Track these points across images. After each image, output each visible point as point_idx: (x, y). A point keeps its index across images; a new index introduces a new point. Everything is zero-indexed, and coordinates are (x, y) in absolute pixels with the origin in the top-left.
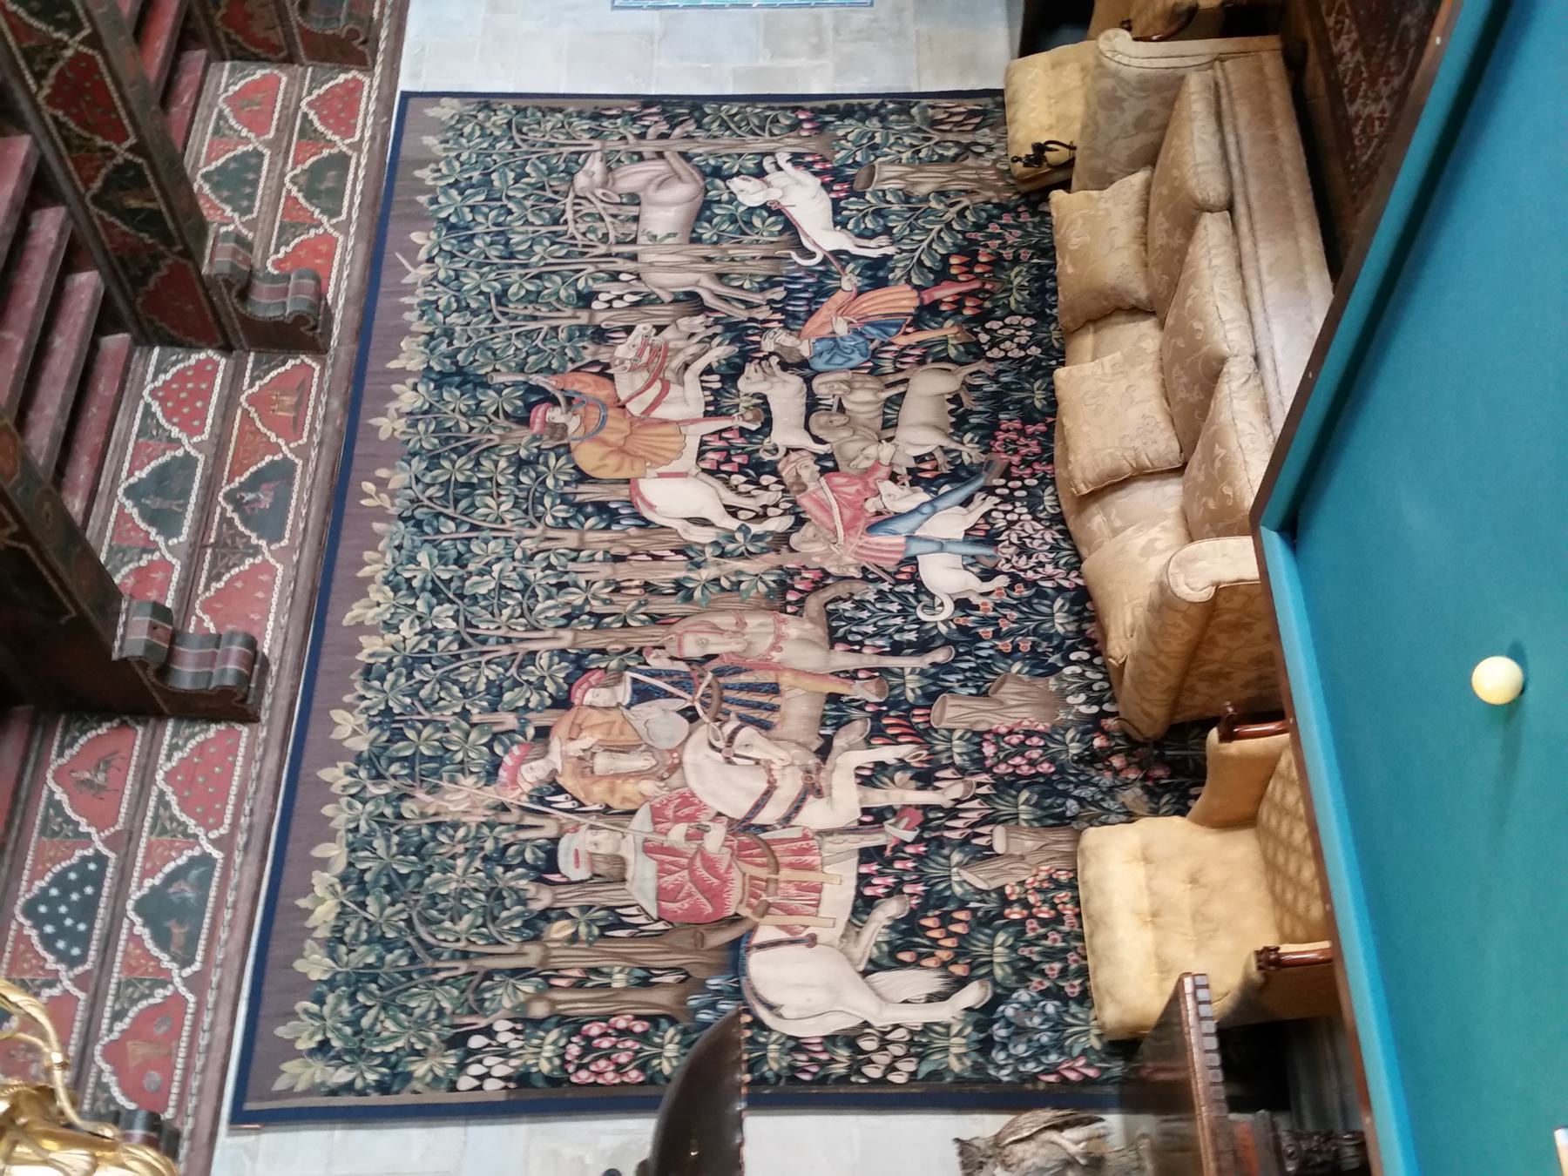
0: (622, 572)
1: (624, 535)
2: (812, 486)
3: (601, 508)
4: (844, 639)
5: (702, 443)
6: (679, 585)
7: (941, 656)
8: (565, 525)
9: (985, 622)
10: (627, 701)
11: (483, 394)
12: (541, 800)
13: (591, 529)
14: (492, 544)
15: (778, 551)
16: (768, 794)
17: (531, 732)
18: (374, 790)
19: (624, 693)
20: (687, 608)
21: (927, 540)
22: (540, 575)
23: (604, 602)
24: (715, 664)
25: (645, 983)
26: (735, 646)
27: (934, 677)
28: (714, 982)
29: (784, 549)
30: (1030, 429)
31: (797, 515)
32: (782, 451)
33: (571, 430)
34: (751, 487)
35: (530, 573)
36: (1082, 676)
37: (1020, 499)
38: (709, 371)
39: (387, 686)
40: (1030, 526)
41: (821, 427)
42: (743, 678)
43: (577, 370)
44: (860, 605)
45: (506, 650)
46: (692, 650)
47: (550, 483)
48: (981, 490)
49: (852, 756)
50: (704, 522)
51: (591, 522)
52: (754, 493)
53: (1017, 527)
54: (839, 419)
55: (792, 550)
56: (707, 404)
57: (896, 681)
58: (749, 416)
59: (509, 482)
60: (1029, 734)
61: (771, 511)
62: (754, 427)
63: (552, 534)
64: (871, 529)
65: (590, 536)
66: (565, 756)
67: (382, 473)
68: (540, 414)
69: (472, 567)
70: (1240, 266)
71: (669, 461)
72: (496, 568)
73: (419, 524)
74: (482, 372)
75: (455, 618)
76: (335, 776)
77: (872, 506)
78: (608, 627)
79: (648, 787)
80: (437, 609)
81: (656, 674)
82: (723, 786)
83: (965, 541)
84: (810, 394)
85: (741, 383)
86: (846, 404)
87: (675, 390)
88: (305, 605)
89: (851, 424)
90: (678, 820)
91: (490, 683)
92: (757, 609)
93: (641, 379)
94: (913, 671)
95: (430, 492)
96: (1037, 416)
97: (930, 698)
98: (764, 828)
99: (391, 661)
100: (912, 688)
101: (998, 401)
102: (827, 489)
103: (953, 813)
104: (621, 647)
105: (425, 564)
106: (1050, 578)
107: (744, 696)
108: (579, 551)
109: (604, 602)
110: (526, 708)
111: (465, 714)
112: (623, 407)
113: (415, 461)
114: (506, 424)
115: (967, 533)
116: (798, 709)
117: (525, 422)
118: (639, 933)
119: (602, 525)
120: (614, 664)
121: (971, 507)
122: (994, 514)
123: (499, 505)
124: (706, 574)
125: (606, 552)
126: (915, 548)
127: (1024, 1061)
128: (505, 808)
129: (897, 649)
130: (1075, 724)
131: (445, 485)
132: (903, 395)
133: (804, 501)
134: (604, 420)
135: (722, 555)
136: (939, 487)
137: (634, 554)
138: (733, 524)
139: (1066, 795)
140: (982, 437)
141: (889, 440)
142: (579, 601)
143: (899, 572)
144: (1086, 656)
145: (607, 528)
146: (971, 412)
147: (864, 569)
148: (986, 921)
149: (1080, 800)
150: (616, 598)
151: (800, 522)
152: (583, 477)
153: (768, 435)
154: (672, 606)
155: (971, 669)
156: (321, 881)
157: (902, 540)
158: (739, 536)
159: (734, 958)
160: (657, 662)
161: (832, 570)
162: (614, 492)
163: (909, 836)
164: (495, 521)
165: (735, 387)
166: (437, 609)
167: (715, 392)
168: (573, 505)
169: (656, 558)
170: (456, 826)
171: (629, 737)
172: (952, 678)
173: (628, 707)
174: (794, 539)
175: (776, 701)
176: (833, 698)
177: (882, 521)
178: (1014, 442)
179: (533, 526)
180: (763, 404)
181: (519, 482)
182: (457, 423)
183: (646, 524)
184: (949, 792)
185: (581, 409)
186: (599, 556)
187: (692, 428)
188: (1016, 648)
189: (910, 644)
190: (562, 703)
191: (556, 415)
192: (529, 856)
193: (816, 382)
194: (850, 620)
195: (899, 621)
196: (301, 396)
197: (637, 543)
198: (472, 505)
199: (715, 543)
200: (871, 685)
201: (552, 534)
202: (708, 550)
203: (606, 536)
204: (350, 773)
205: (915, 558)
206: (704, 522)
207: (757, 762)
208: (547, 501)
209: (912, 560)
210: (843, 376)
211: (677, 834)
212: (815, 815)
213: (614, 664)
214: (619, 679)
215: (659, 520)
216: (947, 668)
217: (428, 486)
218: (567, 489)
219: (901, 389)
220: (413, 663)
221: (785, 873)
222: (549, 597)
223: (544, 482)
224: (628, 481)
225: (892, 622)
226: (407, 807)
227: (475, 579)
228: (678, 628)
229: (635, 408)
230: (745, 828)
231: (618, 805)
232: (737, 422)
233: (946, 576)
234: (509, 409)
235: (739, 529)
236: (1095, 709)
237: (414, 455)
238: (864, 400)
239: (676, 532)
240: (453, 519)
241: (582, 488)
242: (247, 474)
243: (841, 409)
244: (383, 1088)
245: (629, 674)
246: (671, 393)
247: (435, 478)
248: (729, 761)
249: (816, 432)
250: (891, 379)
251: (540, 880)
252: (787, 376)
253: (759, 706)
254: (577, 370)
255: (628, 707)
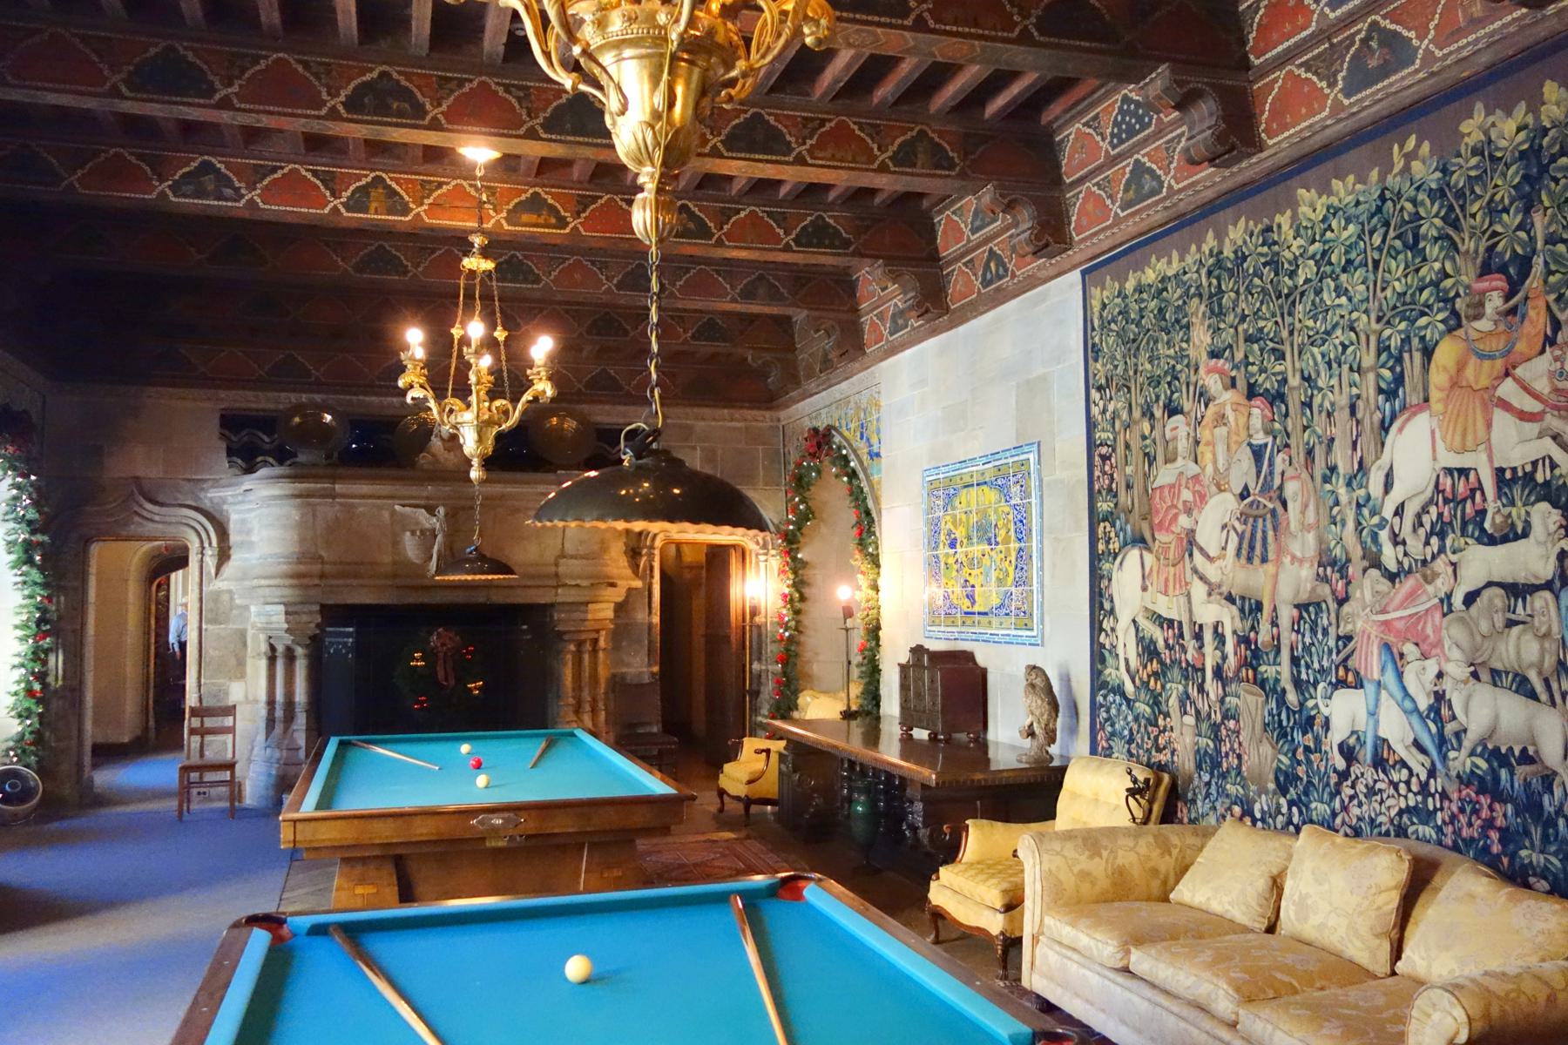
0: (1342, 416)
1: (1372, 405)
2: (1430, 588)
3: (1399, 380)
4: (1301, 617)
5: (1463, 472)
6: (1333, 469)
7: (1292, 697)
8: (1383, 348)
9: (1317, 740)
10: (1254, 442)
11: (1517, 211)
12: (1201, 395)
13: (1379, 376)
14: (1362, 287)
15: (1364, 557)
16: (1208, 557)
17: (1233, 373)
18: (1204, 272)
19: (1260, 439)
20: (1318, 479)
21: (1377, 700)
22: (1337, 342)
23: (1321, 406)
24: (1280, 509)
25: (1129, 487)
26: (1294, 525)
27: (1274, 690)
28: (1129, 528)
29: (1366, 563)
30: (1494, 835)
31: (1397, 575)
32: (1454, 558)
33: (1478, 325)
34: (1428, 527)
35: (1339, 332)
36: (1279, 812)
37: (1425, 802)
38: (1554, 466)
39: (1260, 249)
40: (1395, 804)
41: (1490, 600)
42: (1270, 533)
43: (1548, 308)
44: (1325, 632)
45: (1285, 334)
46: (1291, 488)
47: (1423, 321)
48: (1433, 764)
49: (1230, 619)
50: (1388, 486)
51: (1387, 373)
52: (1422, 532)
53: (1392, 791)
54: (1499, 621)
55: (1365, 571)
56: (1514, 470)
57: (1271, 656)
58: (1499, 519)
59: (1423, 279)
60: (1239, 757)
61: (1400, 548)
62: (1487, 525)
63: (1373, 339)
64: (1387, 647)
65: (1371, 376)
66: (1223, 405)
67: (1426, 147)
68: (1494, 284)
69: (1343, 277)
70: (1167, 993)
71: (1444, 439)
72: (1344, 300)
73: (1379, 210)
74: (1544, 197)
75: (1307, 281)
76: (1210, 242)
77: (1409, 649)
78: (1303, 414)
79: (1209, 470)
80: (1312, 262)
81: (1271, 464)
82: (1214, 521)
83: (1377, 737)
84: (1534, 589)
85: (1544, 506)
86: (1516, 630)
87: (1532, 428)
88: (1303, 152)
89: (1495, 634)
90: (1194, 493)
91: (1261, 330)
92: (1321, 541)
93: (1542, 386)
94: (1278, 673)
95: (1409, 206)
96: (1511, 847)
97: (1262, 683)
98: (1191, 555)
99: (1275, 243)
100: (1267, 670)
101: (1530, 806)
102: (1428, 605)
103: (1201, 689)
104: (1289, 429)
105: (1345, 234)
106: (1345, 808)
107: (1259, 535)
108: (1359, 371)
109: (1321, 406)
110: (1248, 364)
111: (1243, 318)
112: (1507, 374)
113: (1438, 175)
114: (1481, 250)
115: (1385, 740)
116: (1256, 579)
117: (1485, 270)
118: (1146, 476)
119: (1383, 385)
120: (1277, 426)
121: (1414, 750)
122: (1405, 772)
123: (1398, 279)
124: (1342, 491)
125: (1358, 397)
126: (1370, 688)
127: (1108, 711)
128: (1196, 370)
129: (1295, 661)
130: (1246, 795)
131: (1417, 217)
132: (1533, 696)
133: (1409, 583)
134: (1491, 358)
135: (1359, 506)
136: (1434, 721)
137: (1358, 422)
138: (1388, 512)
139: (1212, 775)
140: (1481, 779)
141: (1475, 675)
142: (1320, 383)
143: (1347, 670)
144: (1295, 820)
145: (1380, 391)
146: (1512, 774)
147: (1349, 638)
148: (1156, 702)
149: (1208, 784)
150: (1324, 414)
151: (1392, 577)
152: (1428, 353)
153: (1479, 541)
154: (1319, 468)
155: (1280, 721)
156: (1161, 265)
157: (1376, 676)
158: (1376, 520)
159: (1140, 541)
160: (1280, 459)
161: (1346, 608)
162: (1414, 389)
163: (1189, 657)
164: (1383, 281)
165: (1538, 500)
166: (1312, 262)
167: (1529, 478)
168: (1401, 352)
169: (1354, 444)
170: (1187, 341)
171: (1234, 447)
172: (1274, 705)
173: (1250, 445)
174: (1374, 572)
175: (1257, 561)
176: (1259, 606)
177: (1397, 660)
178: (1475, 812)
179: (1379, 320)
180: (1512, 534)
181: (1421, 290)
182: (1479, 197)
183: (1385, 428)
184: (1212, 687)
185: (1502, 327)
186: (1355, 391)
187: (1484, 457)
188: (1299, 762)
189: (1299, 672)
190: (1252, 392)
191: (1495, 302)
192: (1176, 395)
193: (1547, 594)
194: (1315, 623)
195: (1316, 666)
196: (1487, 17)
197: (1367, 422)
198: (1398, 253)
199: (1369, 498)
200: (1268, 638)
201: (1373, 339)
202: (1362, 492)
203: (1372, 392)
204: (1211, 251)
205: (1362, 687)
206: (1388, 486)
207: (1224, 549)
208: (1403, 326)
209: (1359, 684)
210: (1555, 629)
211: (1187, 495)
212: (1198, 590)
213: (1277, 426)
214: (1267, 432)
215: (1389, 440)
216: (1282, 701)
217: (1414, 201)
218: (1415, 342)
219: (1544, 697)
220: (1274, 263)
221: (1172, 570)
222: (1323, 356)
223: (1423, 314)
224: (1426, 400)
225: (1315, 659)
226: (1196, 300)
227: (1332, 285)
228: (1305, 475)
229: (1508, 389)
230: (1190, 542)
231: (1201, 448)
232: (1492, 506)
233: (1343, 712)
234: (1500, 248)
235: (1383, 519)
236: (1258, 815)
237: (1444, 170)
238: (1523, 651)
239: (1378, 458)
240: (1384, 241)
241: (1417, 356)
242: (1393, 27)
243: (1511, 624)
244: (1094, 345)
245: (1270, 439)
246: (1527, 426)
247: (1423, 203)
248: (1224, 526)
249: (1486, 594)
250: (1555, 686)
251: (1165, 407)
252: (1553, 560)
253: (1252, 548)
254: (1548, 308)
255: (1250, 445)
